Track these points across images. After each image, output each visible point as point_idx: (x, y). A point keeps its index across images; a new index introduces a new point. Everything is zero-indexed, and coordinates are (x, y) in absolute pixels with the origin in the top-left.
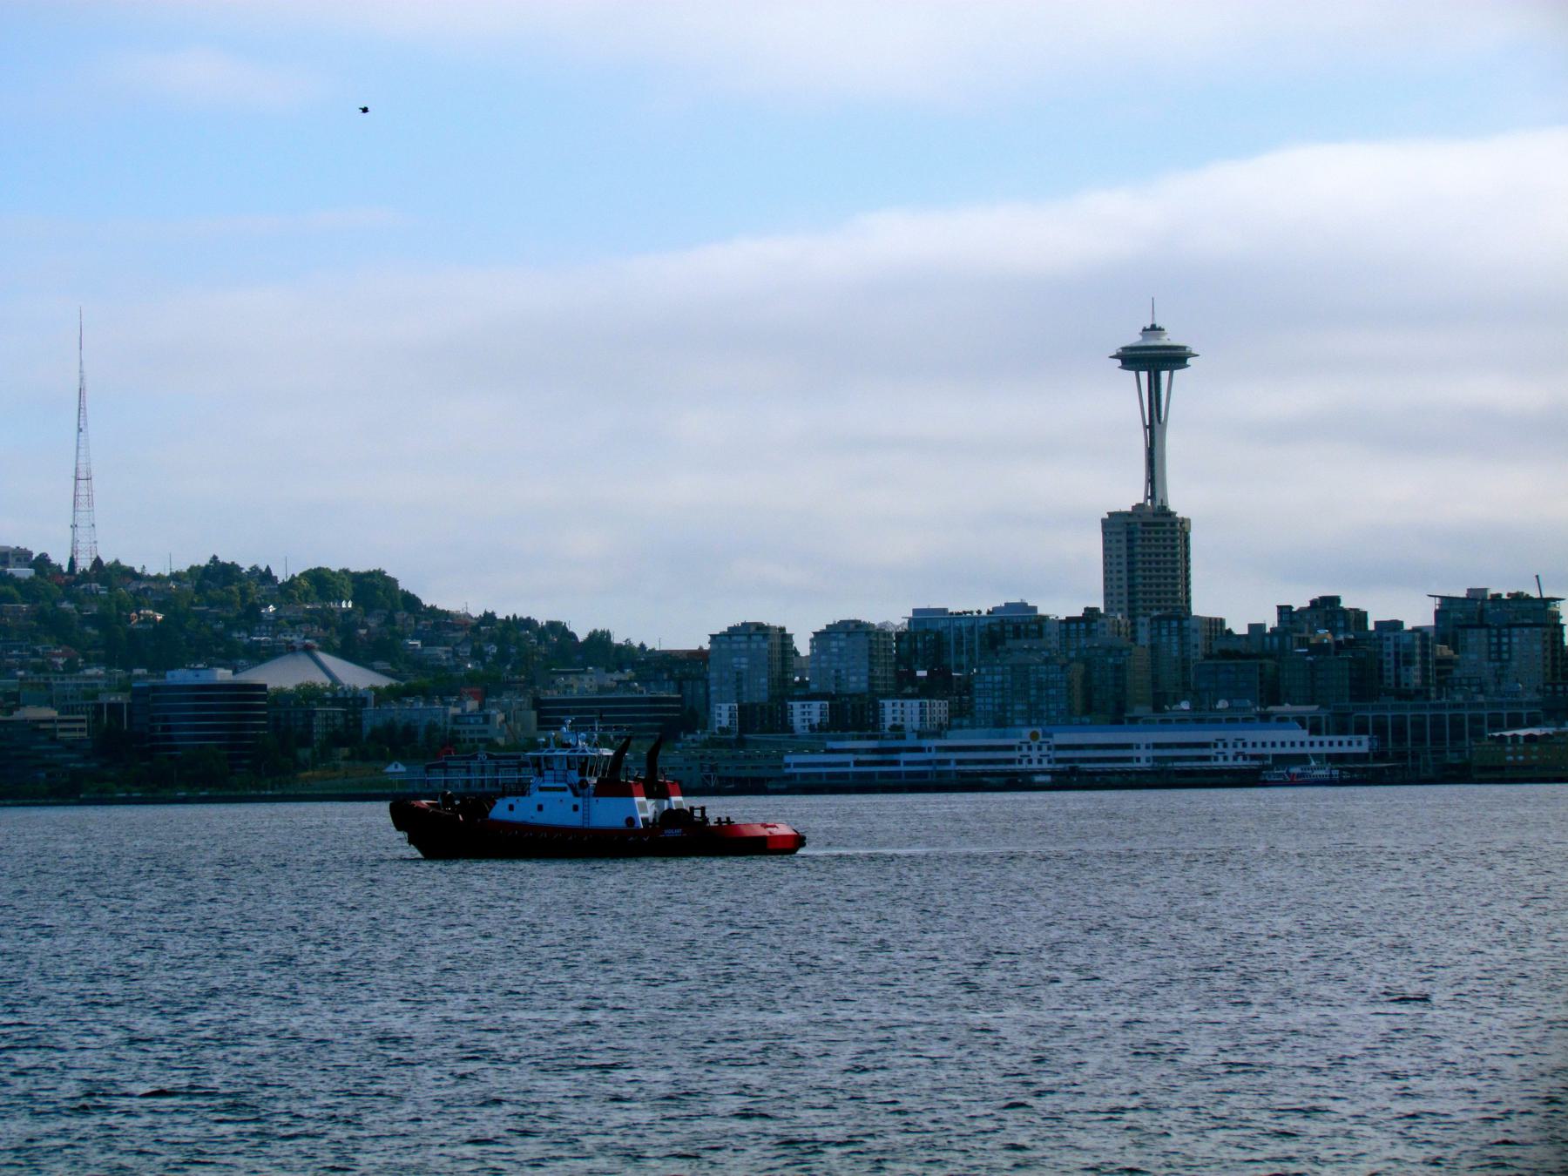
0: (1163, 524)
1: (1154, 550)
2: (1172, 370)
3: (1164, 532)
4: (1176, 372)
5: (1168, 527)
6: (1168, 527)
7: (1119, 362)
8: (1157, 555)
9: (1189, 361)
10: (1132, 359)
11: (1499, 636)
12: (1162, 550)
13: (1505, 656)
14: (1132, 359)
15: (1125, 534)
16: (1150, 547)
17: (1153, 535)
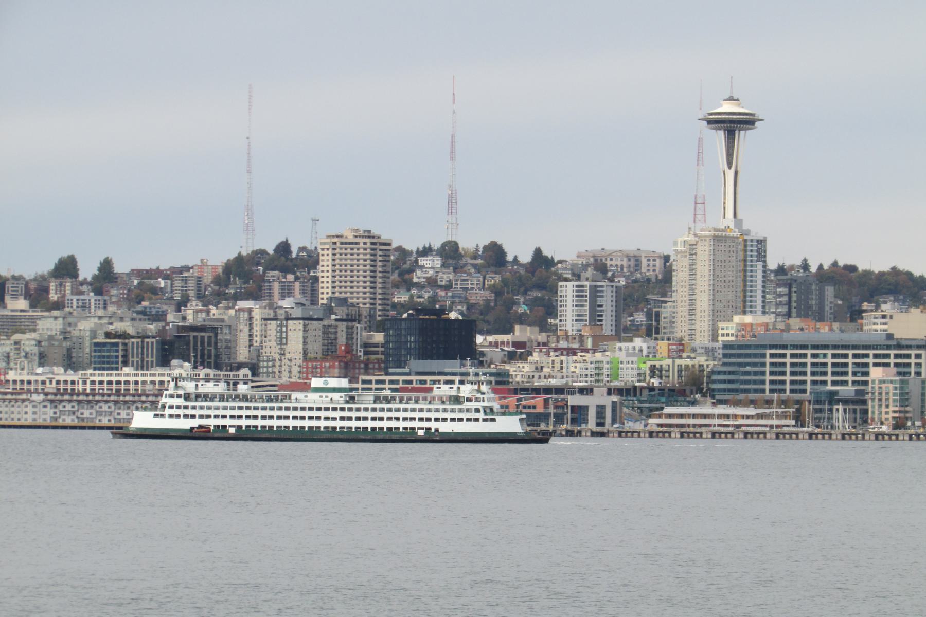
0: (357, 243)
1: (349, 262)
2: (746, 129)
3: (358, 249)
4: (748, 131)
5: (361, 245)
6: (361, 245)
7: (705, 123)
8: (352, 266)
9: (757, 124)
10: (715, 122)
11: (281, 326)
12: (355, 262)
13: (284, 341)
14: (715, 122)
15: (331, 250)
16: (346, 260)
17: (349, 251)
